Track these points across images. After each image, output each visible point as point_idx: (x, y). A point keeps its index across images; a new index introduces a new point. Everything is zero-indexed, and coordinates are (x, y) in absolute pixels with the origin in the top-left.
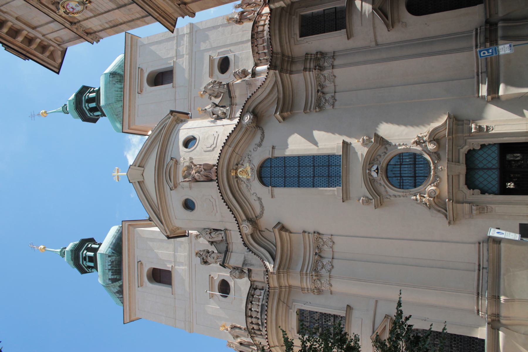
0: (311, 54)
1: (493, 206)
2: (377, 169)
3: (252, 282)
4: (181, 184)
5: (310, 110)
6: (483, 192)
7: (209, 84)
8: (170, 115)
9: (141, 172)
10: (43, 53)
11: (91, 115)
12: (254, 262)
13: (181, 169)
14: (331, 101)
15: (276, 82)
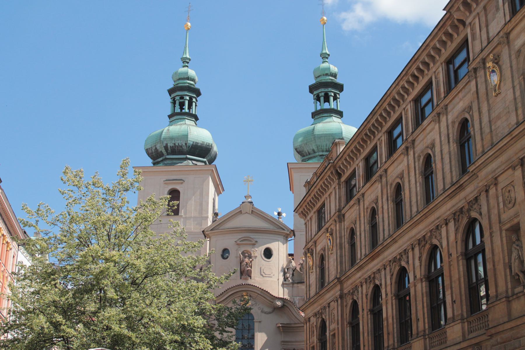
9: (248, 212)
13: (248, 248)
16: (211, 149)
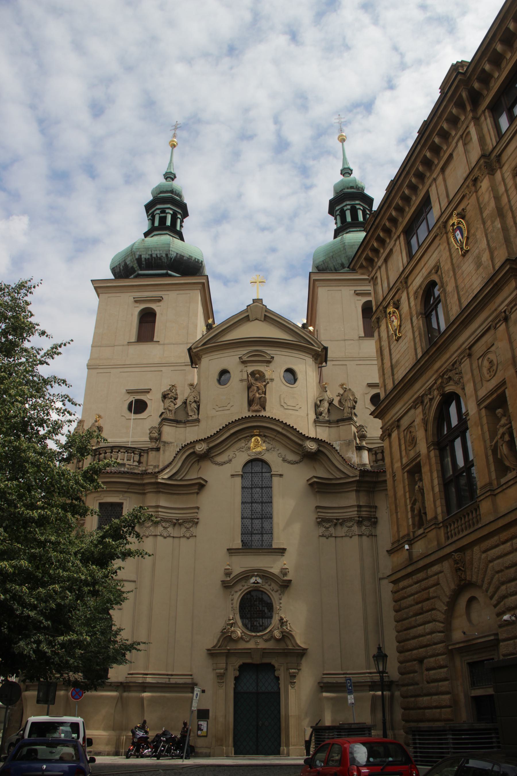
0: (375, 512)
1: (224, 687)
2: (258, 583)
3: (147, 451)
4: (245, 369)
5: (318, 512)
6: (236, 679)
7: (353, 395)
8: (322, 347)
9: (259, 317)
10: (366, 259)
11: (337, 211)
12: (167, 453)
14: (327, 534)
15: (348, 477)
16: (201, 267)
